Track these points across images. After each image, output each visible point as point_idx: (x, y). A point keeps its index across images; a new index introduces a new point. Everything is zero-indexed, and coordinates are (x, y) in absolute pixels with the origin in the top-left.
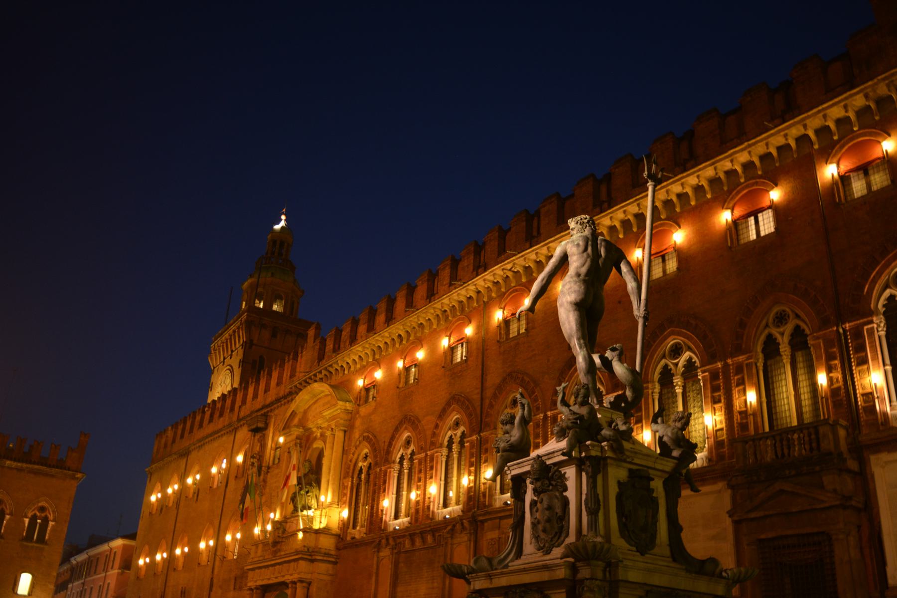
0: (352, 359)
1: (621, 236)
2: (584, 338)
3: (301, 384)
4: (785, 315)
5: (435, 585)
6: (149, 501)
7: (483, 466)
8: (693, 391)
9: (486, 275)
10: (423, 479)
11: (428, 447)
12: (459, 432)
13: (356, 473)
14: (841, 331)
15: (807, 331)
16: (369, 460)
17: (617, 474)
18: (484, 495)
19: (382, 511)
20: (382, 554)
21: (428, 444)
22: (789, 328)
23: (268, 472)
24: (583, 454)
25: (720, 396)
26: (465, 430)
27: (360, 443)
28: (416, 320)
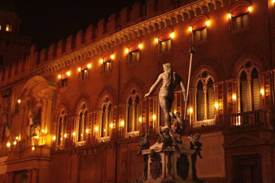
0: (55, 65)
1: (183, 20)
2: (167, 109)
3: (28, 75)
4: (250, 63)
7: (120, 120)
8: (211, 92)
10: (92, 124)
12: (108, 104)
13: (59, 120)
14: (271, 72)
15: (259, 71)
16: (65, 114)
18: (120, 132)
19: (72, 137)
20: (73, 157)
22: (251, 69)
23: (13, 117)
25: (222, 95)
27: (60, 105)
28: (87, 50)
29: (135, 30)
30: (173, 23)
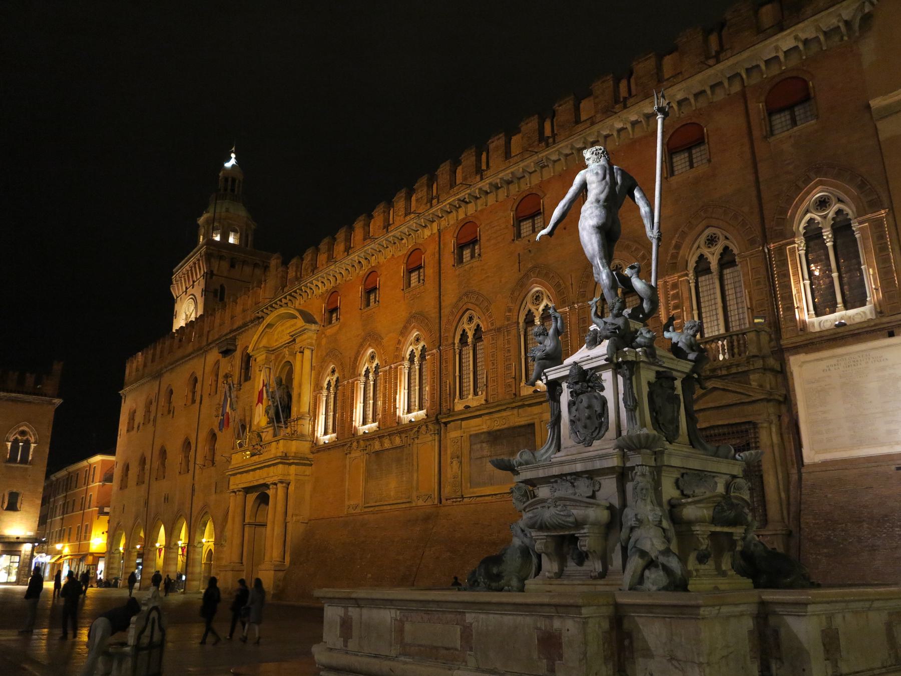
2: (605, 258)
3: (267, 309)
14: (766, 250)
15: (736, 251)
17: (647, 375)
24: (620, 359)
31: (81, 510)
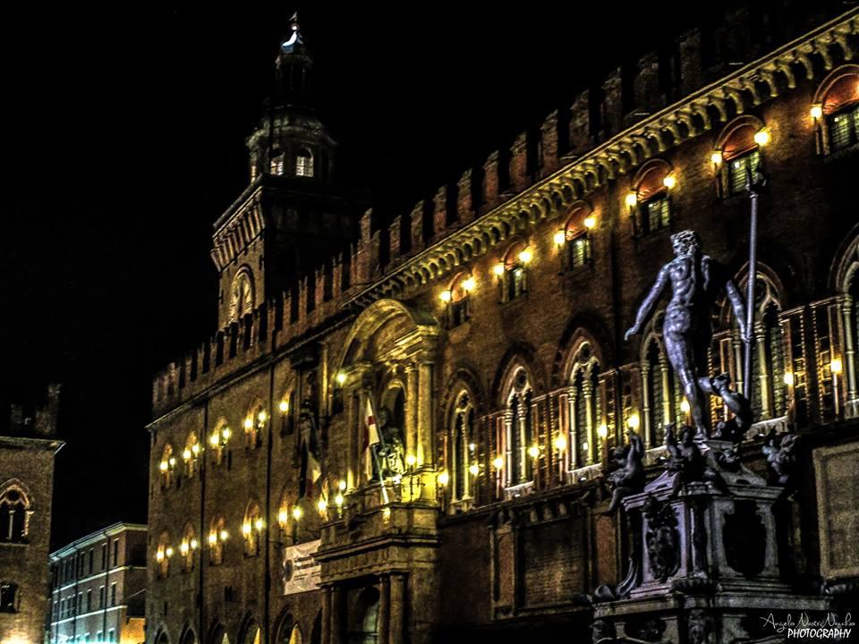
0: (430, 264)
5: (575, 568)
6: (157, 471)
9: (609, 144)
11: (549, 385)
12: (589, 365)
17: (721, 507)
20: (500, 531)
21: (549, 382)
24: (690, 493)
26: (597, 360)
29: (649, 134)
30: (761, 101)
31: (101, 608)
